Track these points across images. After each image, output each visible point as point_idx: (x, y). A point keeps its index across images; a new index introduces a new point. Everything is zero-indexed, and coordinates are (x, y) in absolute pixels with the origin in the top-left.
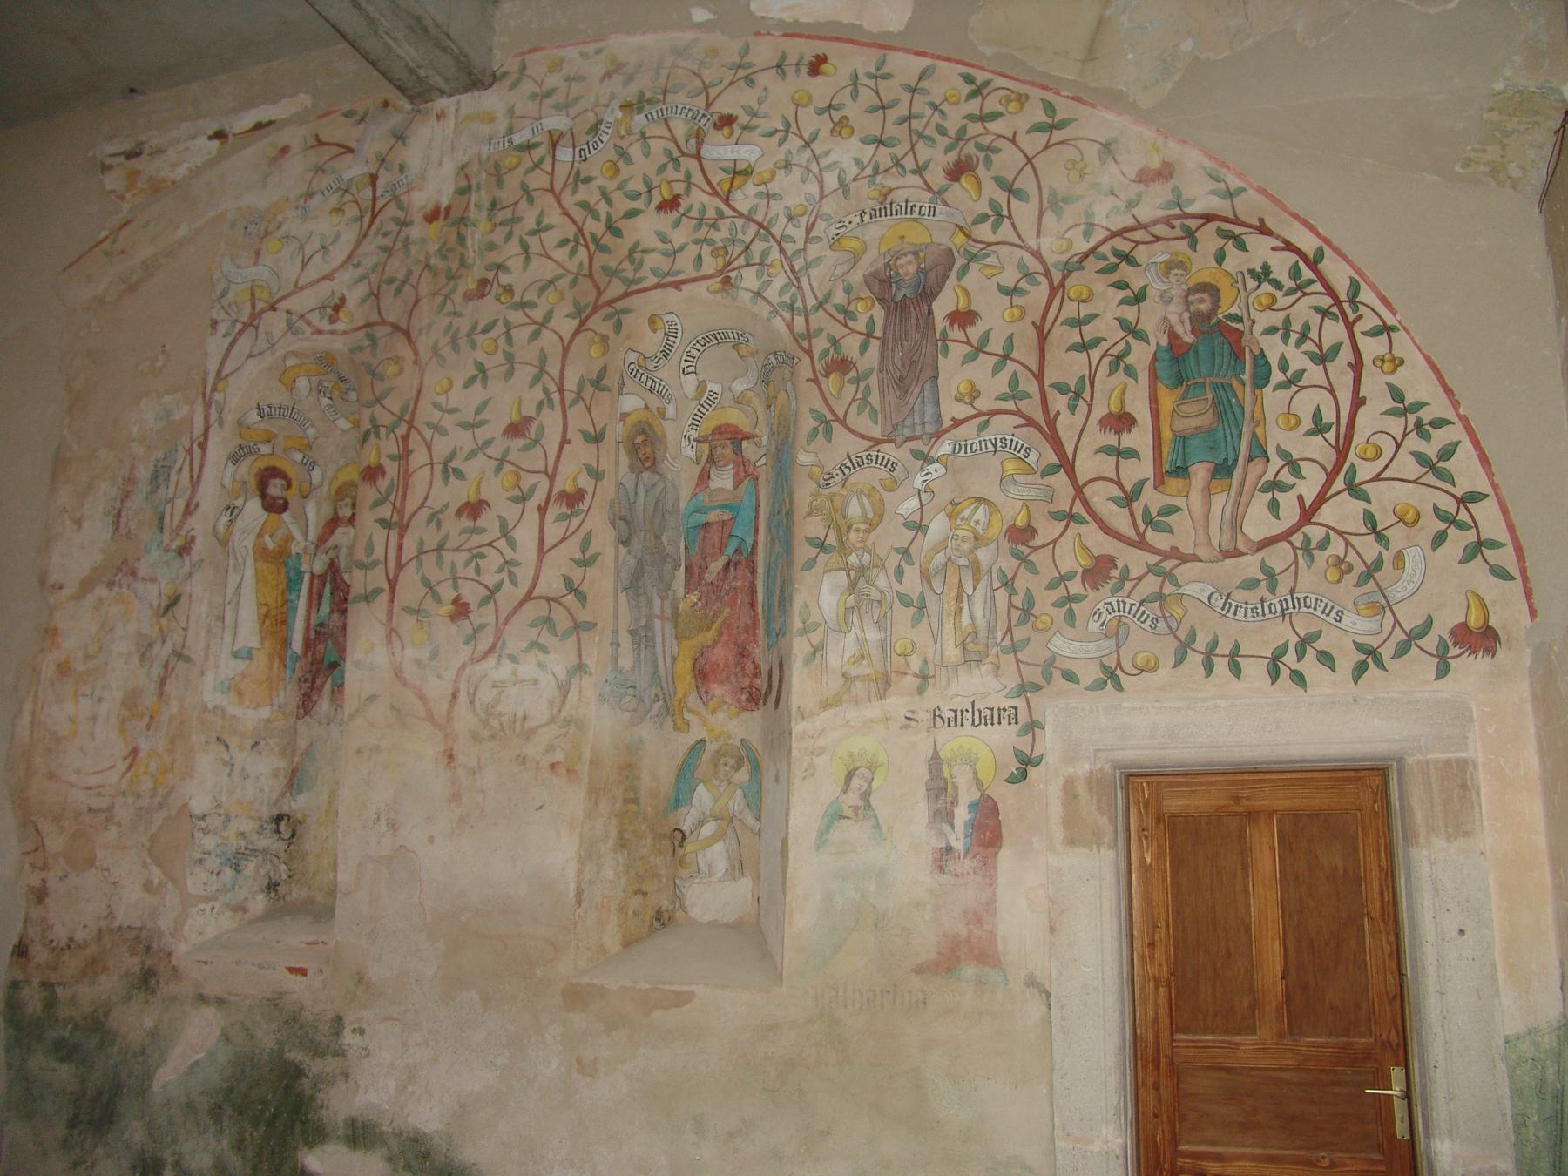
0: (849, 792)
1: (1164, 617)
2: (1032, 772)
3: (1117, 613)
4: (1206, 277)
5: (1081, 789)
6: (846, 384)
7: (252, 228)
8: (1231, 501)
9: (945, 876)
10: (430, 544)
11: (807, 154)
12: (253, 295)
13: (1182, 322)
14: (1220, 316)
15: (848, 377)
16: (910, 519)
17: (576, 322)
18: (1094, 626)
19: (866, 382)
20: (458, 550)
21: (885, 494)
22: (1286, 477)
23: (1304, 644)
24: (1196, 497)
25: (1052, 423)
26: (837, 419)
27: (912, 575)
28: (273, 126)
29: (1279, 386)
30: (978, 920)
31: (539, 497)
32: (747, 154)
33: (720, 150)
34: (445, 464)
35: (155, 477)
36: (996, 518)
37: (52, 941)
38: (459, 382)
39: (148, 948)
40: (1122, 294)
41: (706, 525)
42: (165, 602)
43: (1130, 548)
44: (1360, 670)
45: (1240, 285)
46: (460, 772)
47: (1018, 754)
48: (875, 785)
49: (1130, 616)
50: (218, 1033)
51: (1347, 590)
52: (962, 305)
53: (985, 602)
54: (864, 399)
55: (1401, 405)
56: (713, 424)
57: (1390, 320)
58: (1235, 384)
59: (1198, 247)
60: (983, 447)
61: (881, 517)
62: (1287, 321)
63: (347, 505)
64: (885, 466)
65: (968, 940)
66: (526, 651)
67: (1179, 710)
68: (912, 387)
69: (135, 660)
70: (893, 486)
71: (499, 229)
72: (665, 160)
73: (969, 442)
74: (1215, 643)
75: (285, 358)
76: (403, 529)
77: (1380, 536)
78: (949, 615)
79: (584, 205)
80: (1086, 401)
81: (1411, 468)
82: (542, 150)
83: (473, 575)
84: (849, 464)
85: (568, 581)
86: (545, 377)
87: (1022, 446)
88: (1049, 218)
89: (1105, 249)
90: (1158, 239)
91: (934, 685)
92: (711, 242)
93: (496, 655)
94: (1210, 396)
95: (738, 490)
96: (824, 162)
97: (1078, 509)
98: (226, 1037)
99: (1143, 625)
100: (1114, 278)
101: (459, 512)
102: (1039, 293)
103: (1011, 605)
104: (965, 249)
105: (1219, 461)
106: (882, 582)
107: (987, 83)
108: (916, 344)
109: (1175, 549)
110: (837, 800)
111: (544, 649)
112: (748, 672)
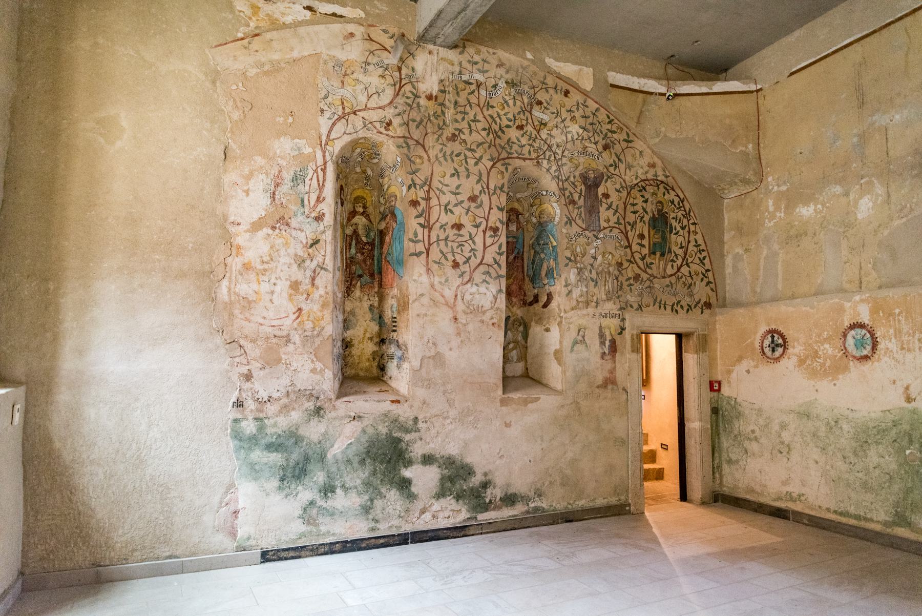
2: (623, 331)
4: (661, 200)
5: (635, 337)
7: (337, 68)
10: (442, 237)
11: (563, 125)
12: (343, 103)
17: (491, 163)
18: (636, 293)
20: (453, 241)
22: (675, 258)
23: (679, 302)
24: (657, 260)
25: (627, 233)
27: (594, 272)
28: (342, 20)
29: (674, 234)
31: (483, 227)
32: (545, 117)
33: (537, 113)
34: (446, 206)
35: (295, 179)
37: (258, 399)
38: (448, 175)
39: (318, 398)
40: (643, 199)
42: (310, 242)
44: (688, 311)
46: (460, 325)
47: (621, 327)
50: (360, 429)
51: (685, 290)
52: (606, 192)
54: (580, 215)
55: (697, 246)
57: (696, 222)
62: (677, 217)
63: (360, 207)
66: (482, 283)
69: (295, 267)
70: (588, 244)
71: (459, 114)
72: (520, 110)
74: (661, 301)
75: (361, 139)
76: (430, 229)
77: (692, 278)
79: (492, 117)
81: (698, 262)
82: (473, 87)
83: (460, 252)
85: (495, 260)
86: (482, 181)
88: (628, 170)
89: (640, 184)
90: (651, 185)
92: (533, 147)
96: (568, 130)
97: (632, 260)
98: (364, 431)
100: (641, 194)
101: (453, 227)
102: (625, 193)
106: (586, 274)
107: (613, 120)
111: (487, 282)
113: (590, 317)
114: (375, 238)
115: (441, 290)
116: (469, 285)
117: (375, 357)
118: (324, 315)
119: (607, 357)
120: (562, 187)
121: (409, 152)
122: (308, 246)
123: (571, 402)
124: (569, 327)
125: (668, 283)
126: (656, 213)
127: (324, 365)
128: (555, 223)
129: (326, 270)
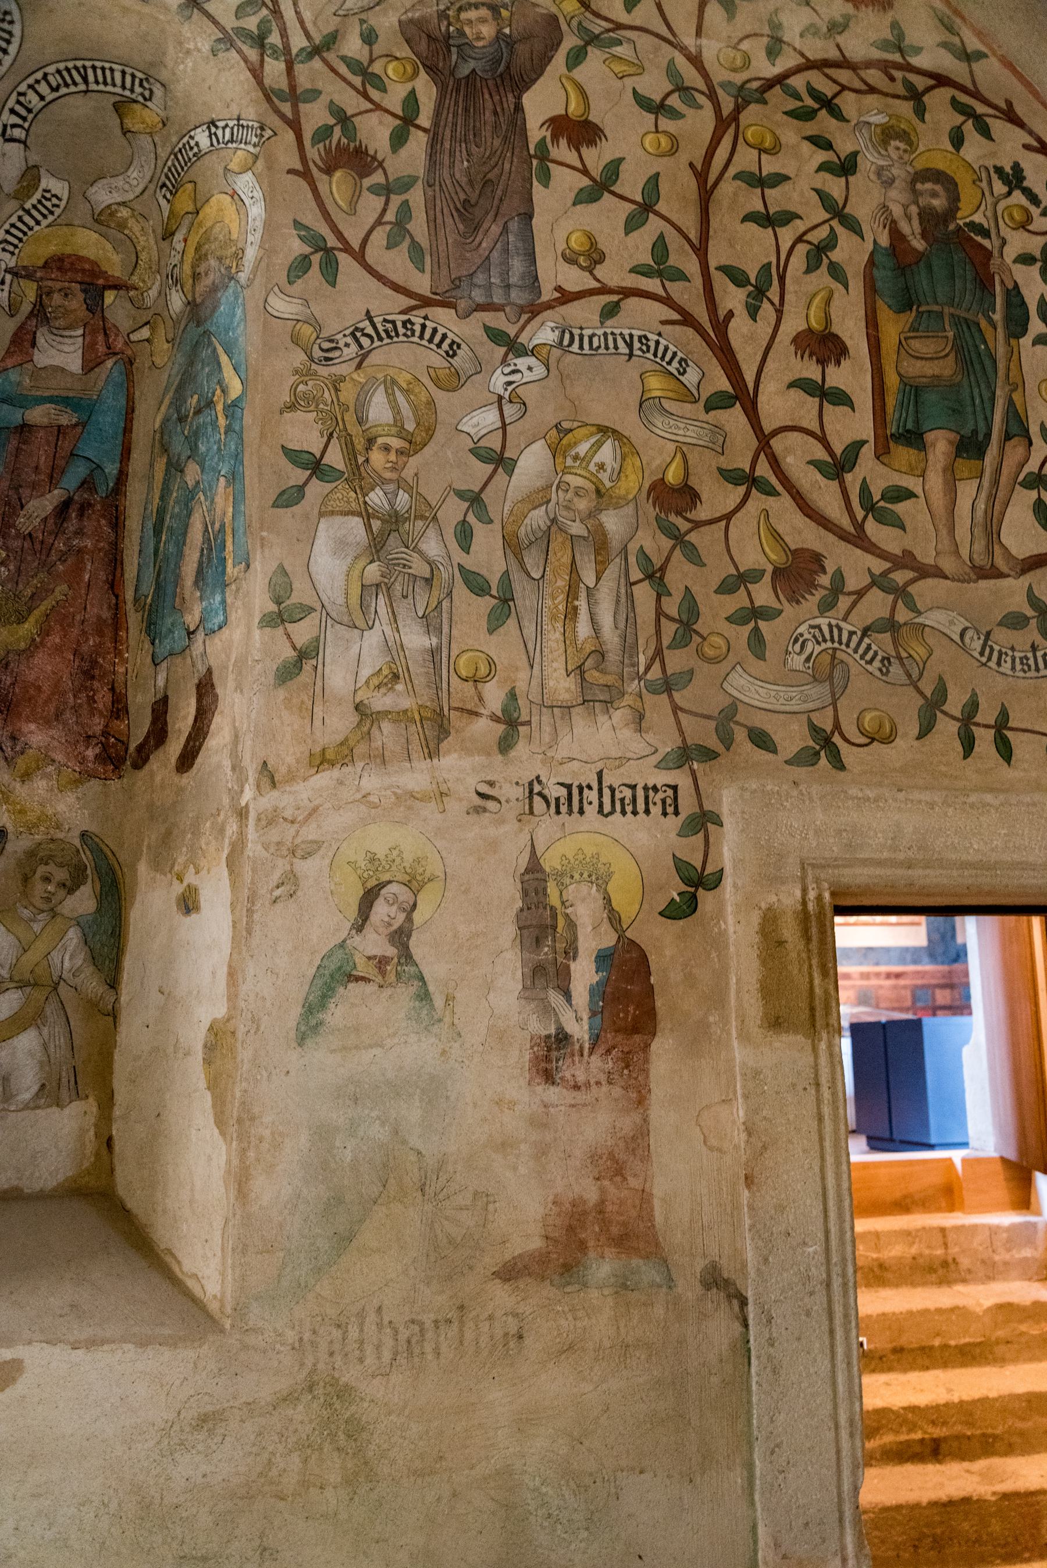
0: (368, 929)
1: (899, 658)
3: (829, 644)
4: (940, 163)
5: (790, 931)
6: (366, 193)
8: (983, 495)
9: (553, 1089)
13: (909, 218)
14: (961, 223)
15: (367, 182)
16: (481, 444)
18: (797, 661)
19: (403, 197)
21: (439, 395)
24: (935, 480)
25: (721, 325)
26: (347, 249)
30: (619, 1171)
36: (633, 462)
40: (822, 156)
41: (24, 429)
43: (843, 543)
45: (984, 184)
47: (681, 866)
48: (417, 916)
49: (850, 651)
52: (574, 108)
53: (618, 602)
54: (401, 226)
56: (53, 249)
58: (983, 324)
59: (927, 116)
60: (611, 345)
61: (430, 432)
64: (439, 346)
65: (600, 1208)
67: (932, 805)
68: (485, 226)
70: (453, 382)
73: (587, 332)
74: (973, 706)
78: (554, 618)
80: (772, 303)
84: (370, 330)
87: (675, 354)
89: (797, 82)
90: (872, 90)
91: (530, 738)
94: (951, 334)
95: (92, 375)
97: (763, 469)
99: (868, 667)
100: (811, 128)
103: (659, 613)
104: (580, 23)
105: (967, 431)
106: (432, 546)
108: (493, 154)
109: (908, 554)
110: (342, 945)
112: (101, 706)
113: (455, 808)
119: (573, 1070)
120: (283, 84)
123: (283, 1385)
124: (291, 882)
125: (1019, 603)
126: (911, 229)
128: (243, 277)
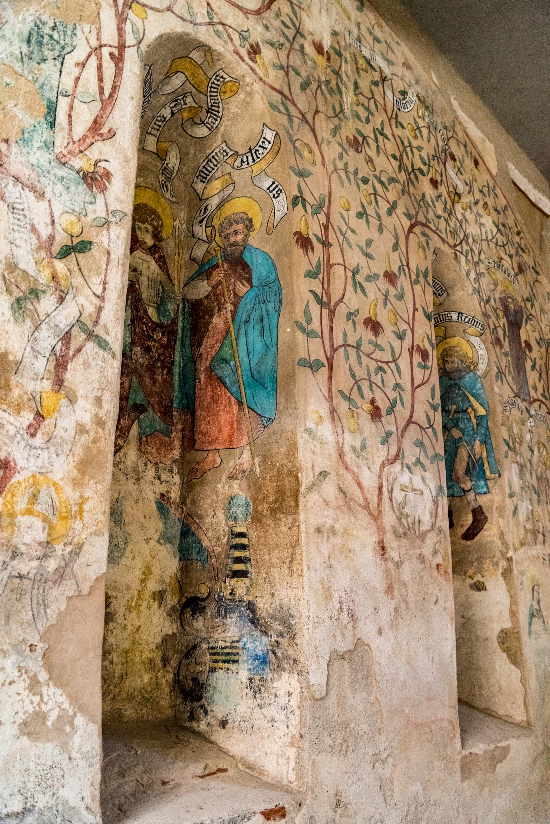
42: (62, 239)
93: (400, 462)
111: (423, 467)
114: (176, 317)
115: (356, 470)
116: (397, 467)
117: (170, 653)
118: (83, 500)
121: (292, 127)
122: (56, 249)
127: (73, 699)
128: (479, 373)
129: (102, 344)
